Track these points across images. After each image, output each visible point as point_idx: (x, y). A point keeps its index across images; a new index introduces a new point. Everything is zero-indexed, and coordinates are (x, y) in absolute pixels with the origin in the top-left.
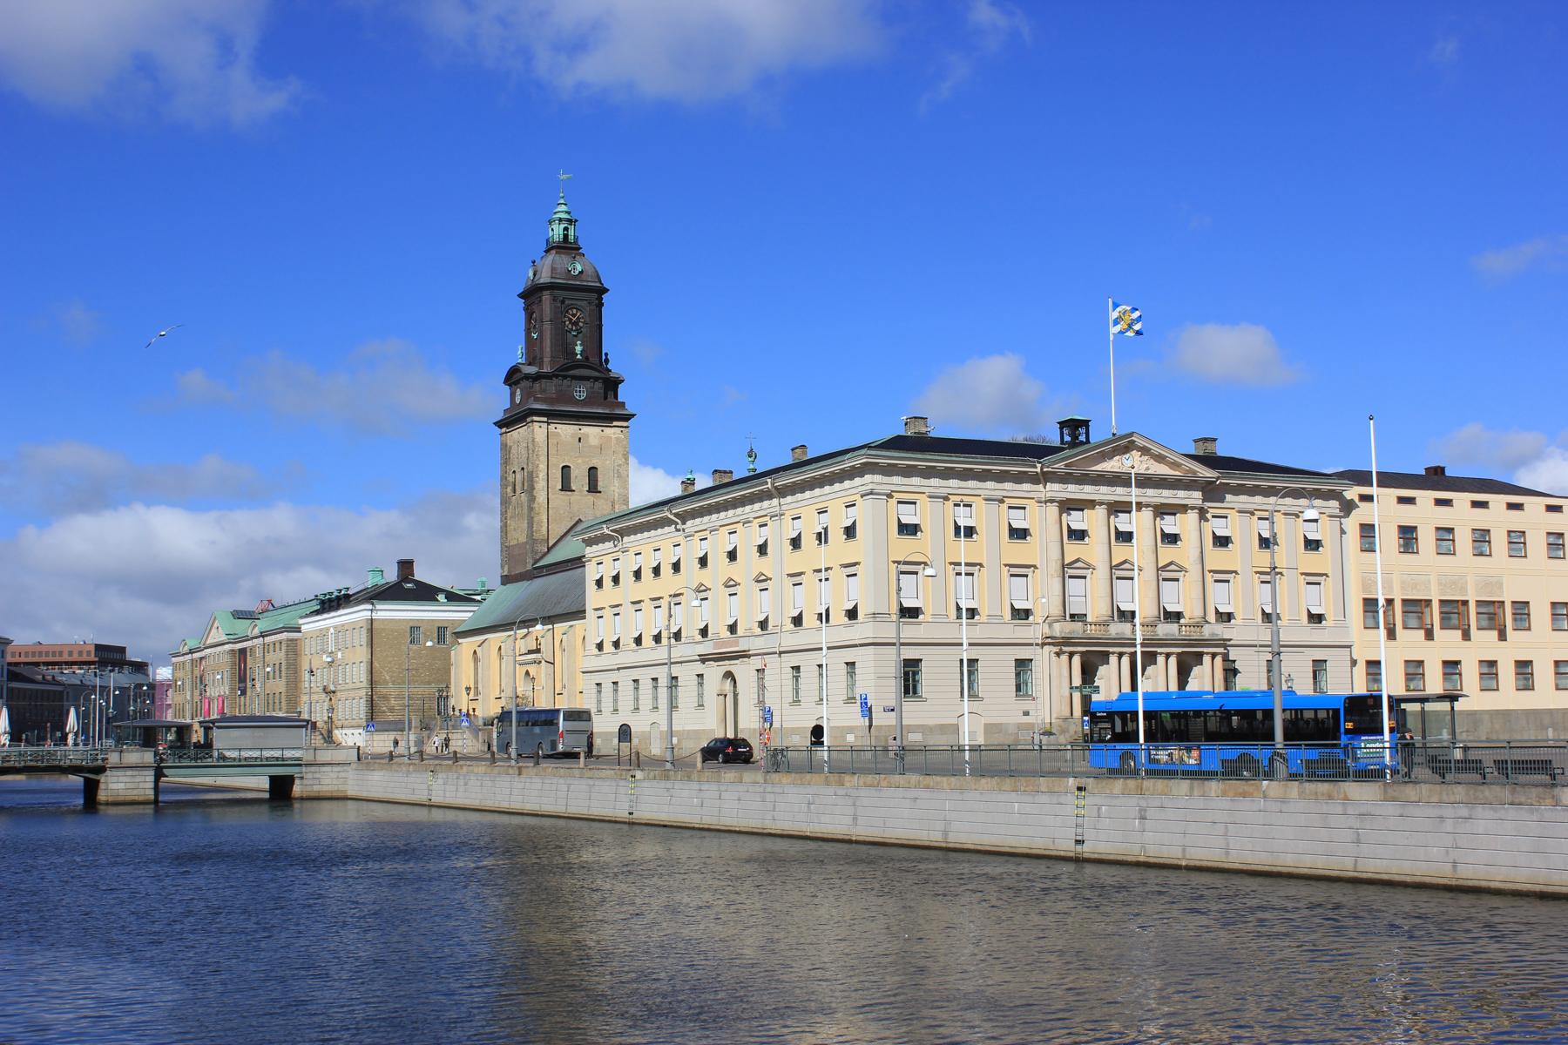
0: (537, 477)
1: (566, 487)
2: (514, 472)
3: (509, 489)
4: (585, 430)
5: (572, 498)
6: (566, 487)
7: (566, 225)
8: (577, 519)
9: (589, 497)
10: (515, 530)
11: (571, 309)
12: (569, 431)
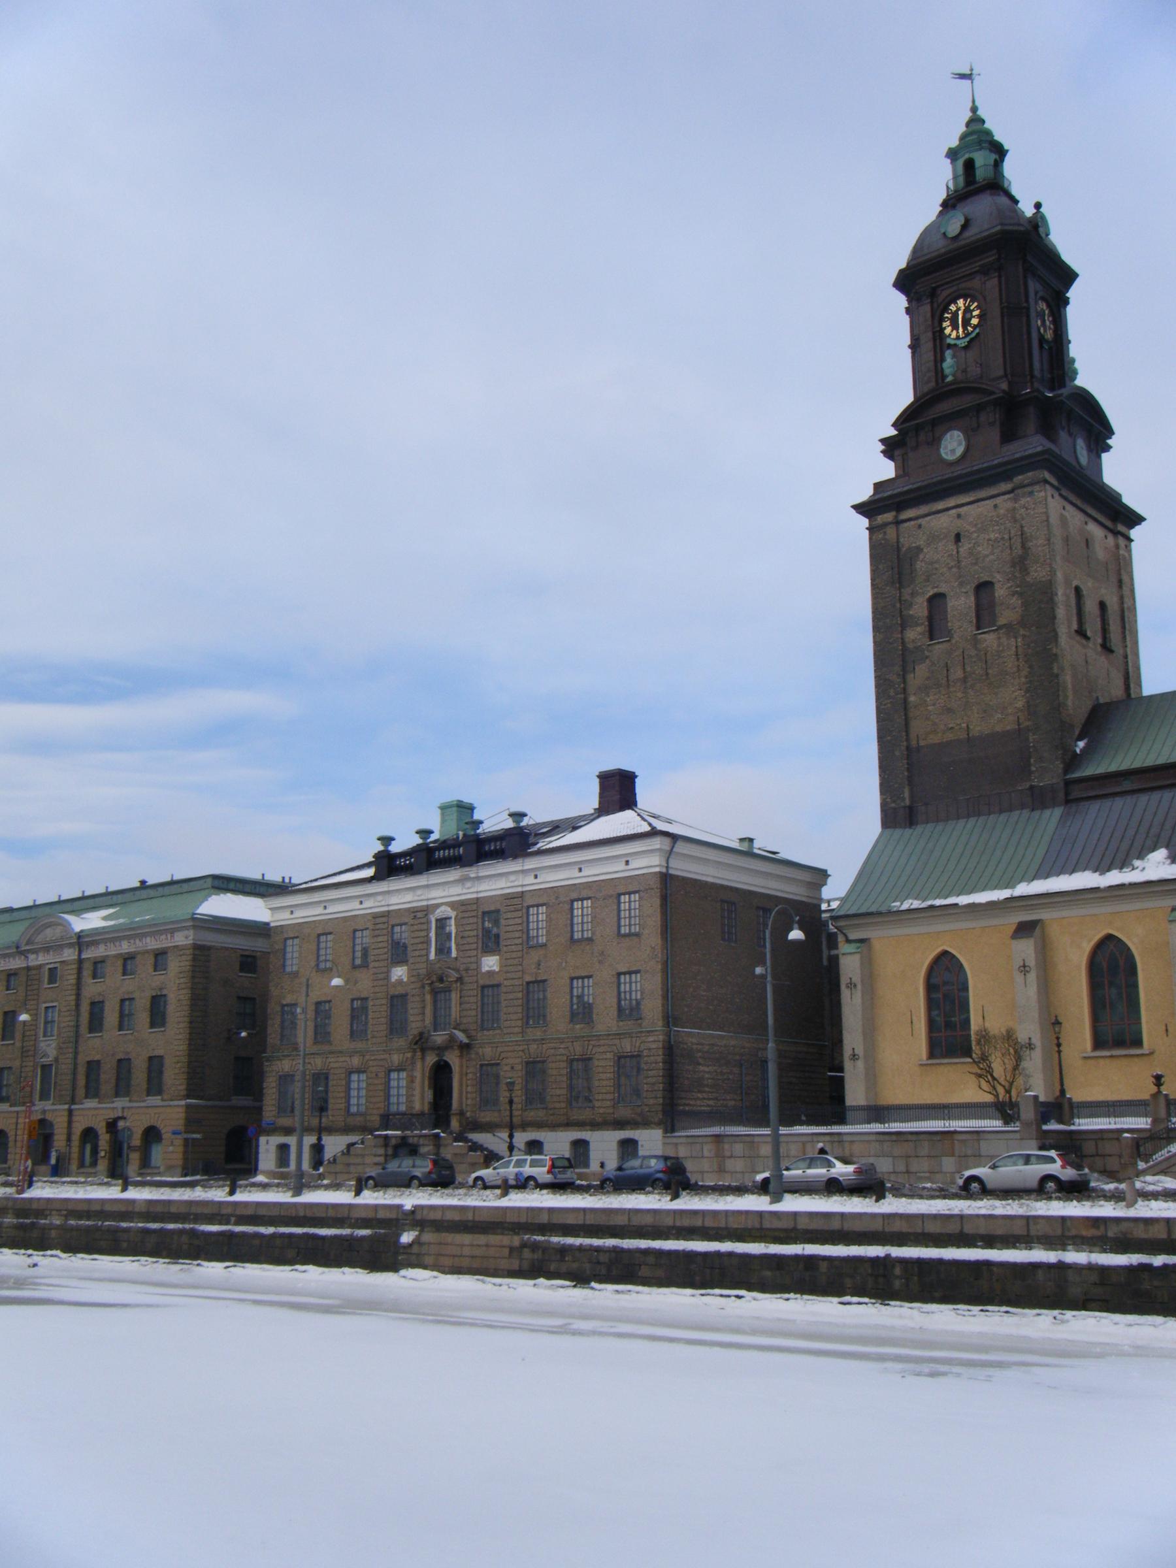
0: (1056, 594)
3: (915, 634)
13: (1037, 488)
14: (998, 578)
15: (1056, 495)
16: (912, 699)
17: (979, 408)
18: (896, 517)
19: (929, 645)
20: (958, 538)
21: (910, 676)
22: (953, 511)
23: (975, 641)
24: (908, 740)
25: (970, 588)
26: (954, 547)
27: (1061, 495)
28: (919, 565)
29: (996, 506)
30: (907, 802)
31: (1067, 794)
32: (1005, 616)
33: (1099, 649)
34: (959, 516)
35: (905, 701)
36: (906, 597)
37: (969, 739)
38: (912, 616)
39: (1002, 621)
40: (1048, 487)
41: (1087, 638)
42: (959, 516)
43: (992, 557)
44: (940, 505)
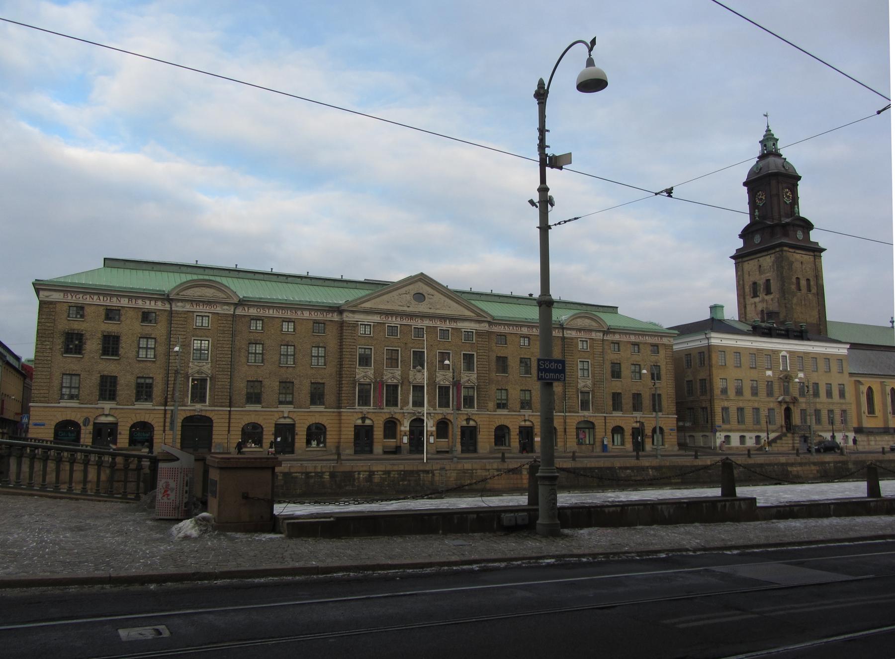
14: (811, 279)
20: (802, 262)
26: (801, 265)
29: (810, 258)
34: (802, 257)
44: (797, 251)
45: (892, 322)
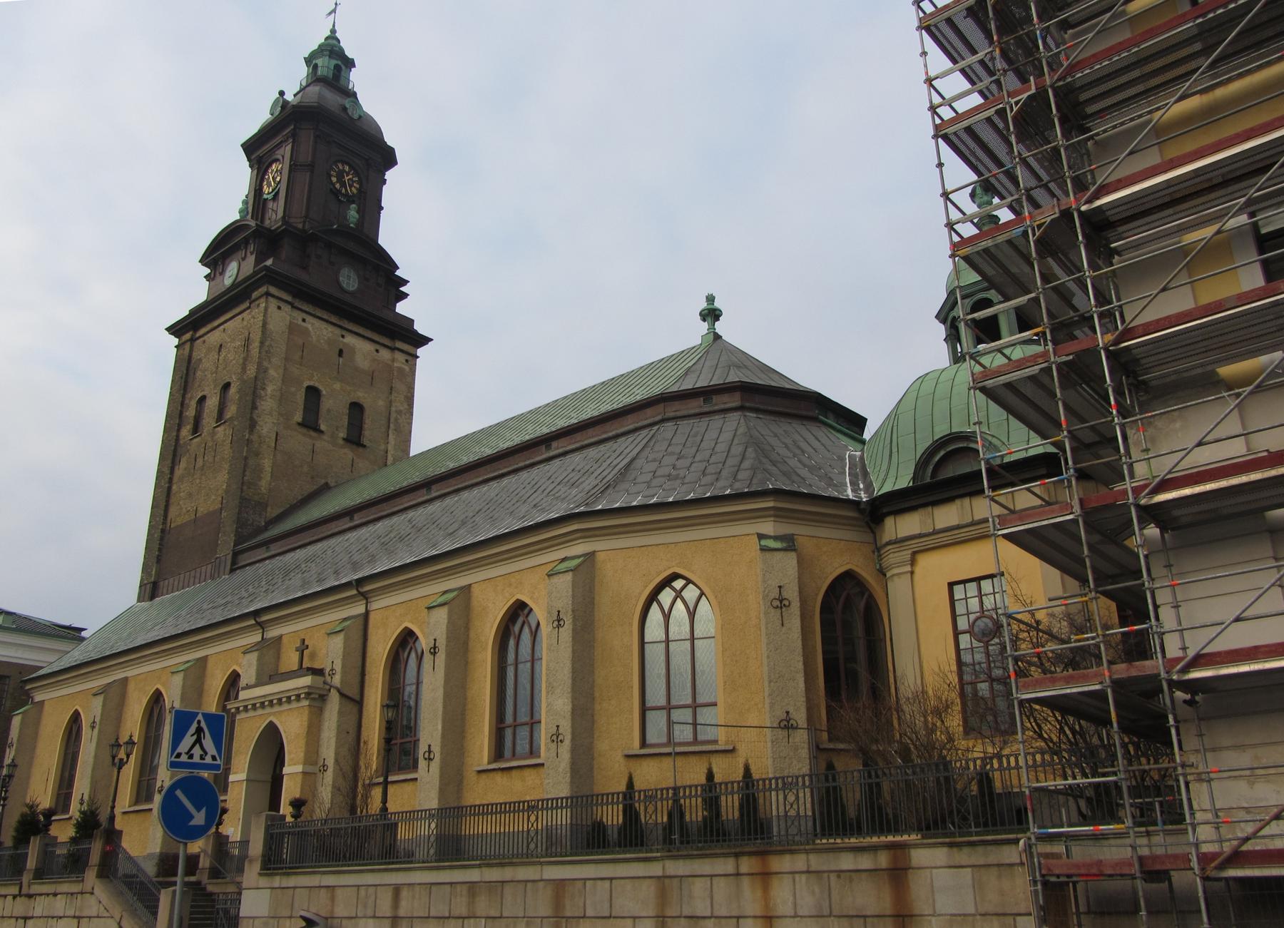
0: (264, 389)
1: (310, 424)
2: (203, 399)
3: (186, 432)
4: (350, 340)
5: (318, 444)
6: (310, 424)
7: (339, 63)
8: (323, 481)
9: (346, 450)
10: (190, 495)
11: (344, 163)
12: (325, 332)
13: (263, 300)
15: (287, 308)
16: (174, 487)
17: (246, 242)
18: (192, 335)
19: (191, 439)
20: (221, 345)
21: (177, 467)
22: (222, 327)
23: (213, 434)
24: (164, 523)
25: (218, 390)
27: (293, 307)
28: (199, 373)
30: (153, 579)
31: (234, 562)
32: (231, 411)
33: (341, 442)
35: (169, 489)
36: (187, 401)
37: (195, 520)
38: (187, 416)
39: (228, 415)
40: (271, 299)
41: (322, 432)
42: (224, 330)
43: (234, 362)
45: (711, 314)
